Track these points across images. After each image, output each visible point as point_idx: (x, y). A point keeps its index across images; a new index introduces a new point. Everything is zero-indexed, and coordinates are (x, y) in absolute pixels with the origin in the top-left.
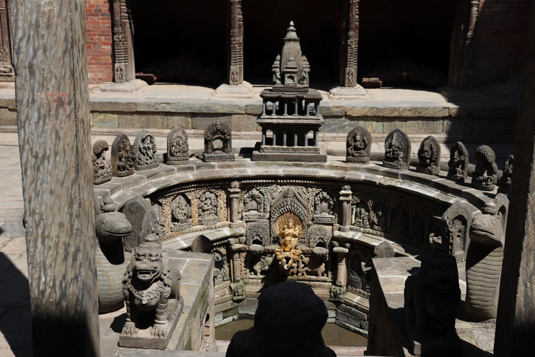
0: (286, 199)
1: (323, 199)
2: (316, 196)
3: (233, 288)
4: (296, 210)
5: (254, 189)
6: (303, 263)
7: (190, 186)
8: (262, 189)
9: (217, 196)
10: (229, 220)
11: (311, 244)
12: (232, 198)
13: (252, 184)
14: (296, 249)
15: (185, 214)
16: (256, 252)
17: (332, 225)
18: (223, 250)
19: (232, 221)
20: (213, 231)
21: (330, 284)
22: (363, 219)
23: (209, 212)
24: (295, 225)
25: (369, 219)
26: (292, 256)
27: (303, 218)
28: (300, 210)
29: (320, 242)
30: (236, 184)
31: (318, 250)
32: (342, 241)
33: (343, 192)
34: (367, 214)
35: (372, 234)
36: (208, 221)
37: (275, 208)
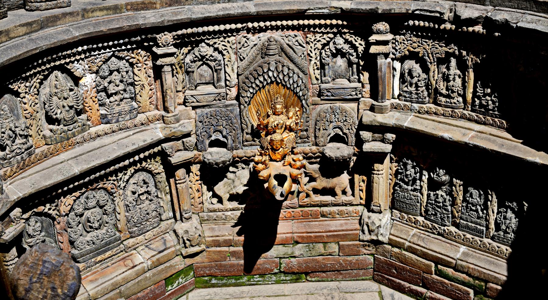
0: (267, 58)
1: (339, 53)
2: (323, 48)
3: (180, 232)
4: (286, 79)
5: (203, 44)
6: (306, 175)
7: (75, 50)
8: (220, 43)
9: (132, 65)
10: (161, 106)
11: (321, 140)
12: (162, 66)
13: (198, 34)
14: (293, 152)
15: (71, 107)
16: (217, 164)
17: (357, 100)
18: (157, 166)
19: (166, 109)
20: (131, 133)
21: (360, 208)
22: (417, 86)
23: (117, 98)
24: (287, 107)
25: (428, 86)
26: (287, 171)
27: (301, 94)
28: (295, 76)
29: (337, 135)
30: (166, 37)
31: (335, 150)
32: (380, 130)
33: (373, 38)
34: (424, 76)
35: (436, 114)
36: (120, 114)
37: (247, 78)
